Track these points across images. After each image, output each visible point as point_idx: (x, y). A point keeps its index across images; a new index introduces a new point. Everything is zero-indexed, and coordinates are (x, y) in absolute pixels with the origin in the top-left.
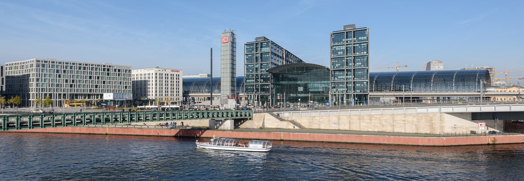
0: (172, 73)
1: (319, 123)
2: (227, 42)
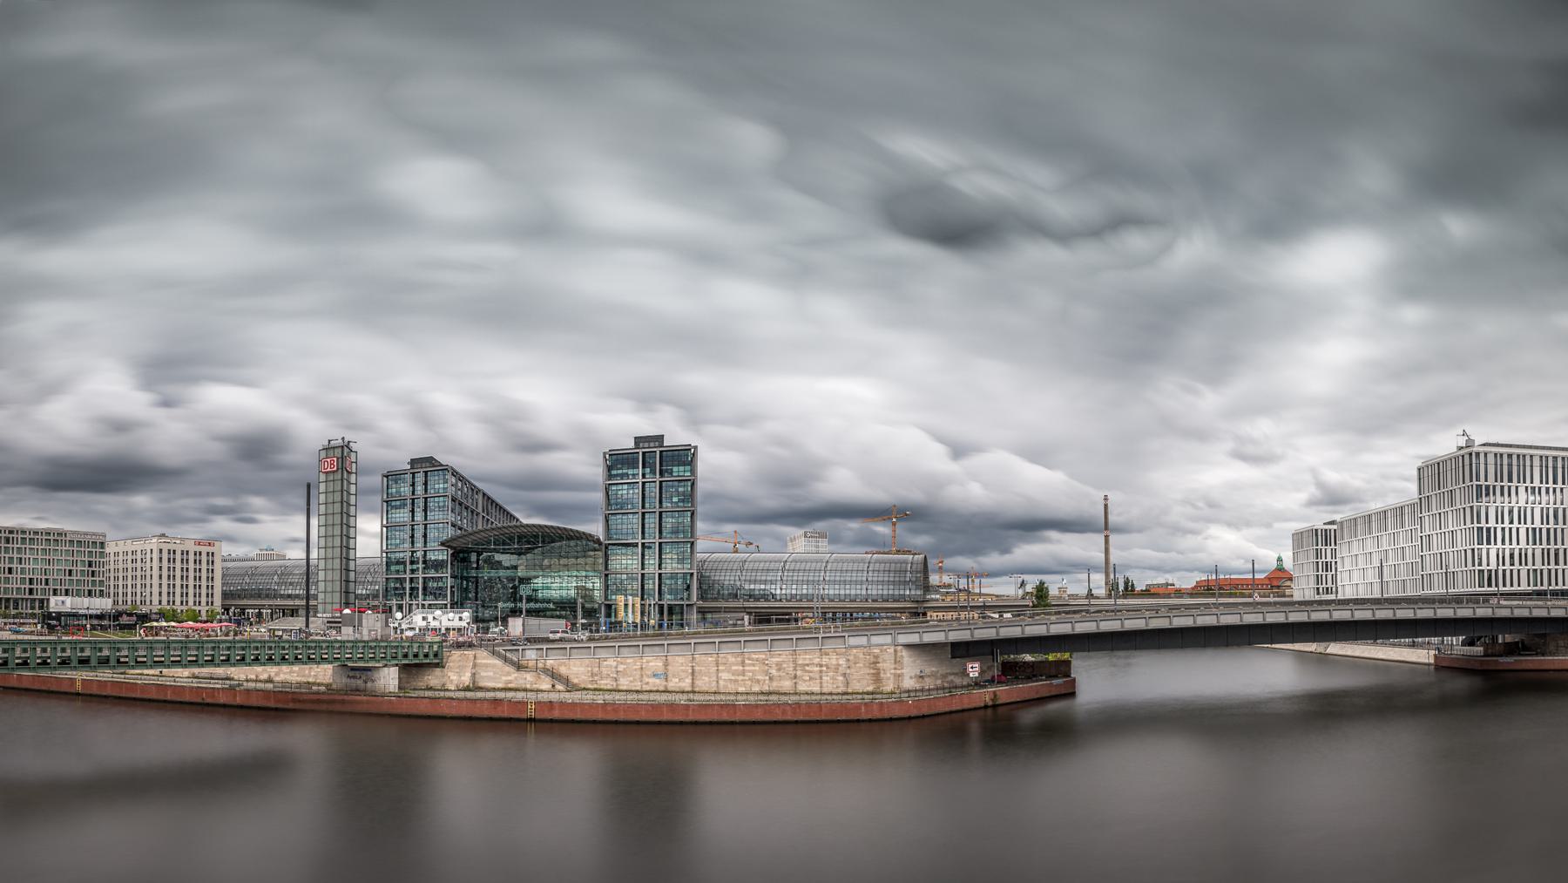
0: (198, 548)
1: (615, 676)
2: (334, 472)
